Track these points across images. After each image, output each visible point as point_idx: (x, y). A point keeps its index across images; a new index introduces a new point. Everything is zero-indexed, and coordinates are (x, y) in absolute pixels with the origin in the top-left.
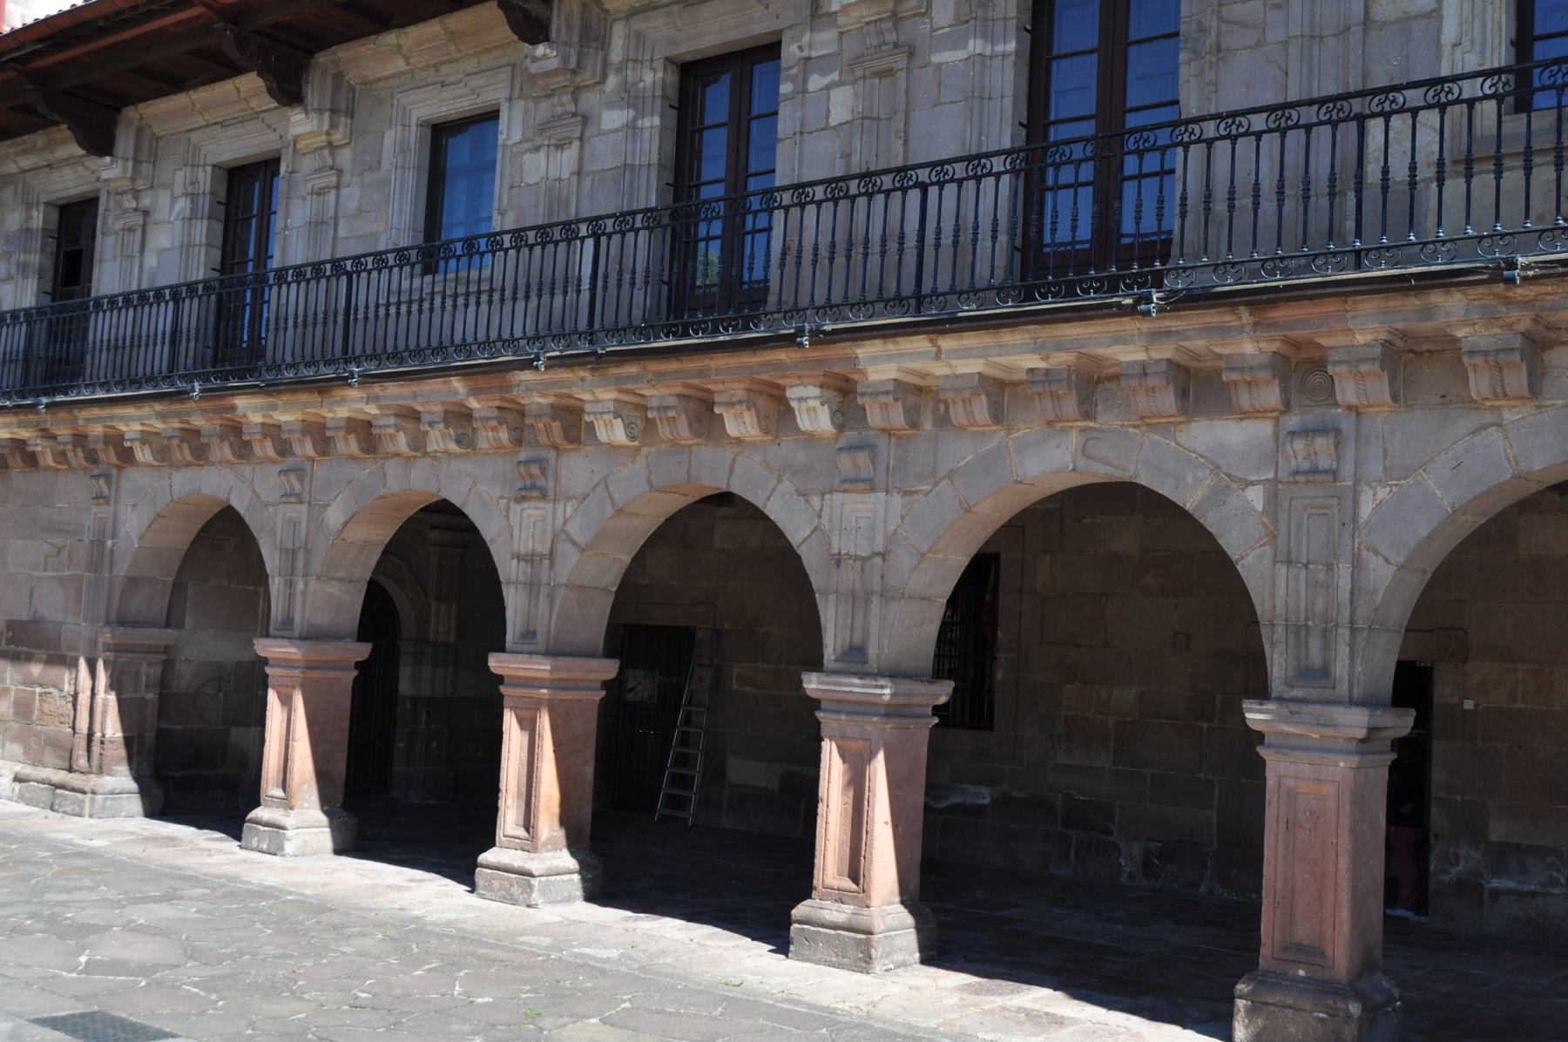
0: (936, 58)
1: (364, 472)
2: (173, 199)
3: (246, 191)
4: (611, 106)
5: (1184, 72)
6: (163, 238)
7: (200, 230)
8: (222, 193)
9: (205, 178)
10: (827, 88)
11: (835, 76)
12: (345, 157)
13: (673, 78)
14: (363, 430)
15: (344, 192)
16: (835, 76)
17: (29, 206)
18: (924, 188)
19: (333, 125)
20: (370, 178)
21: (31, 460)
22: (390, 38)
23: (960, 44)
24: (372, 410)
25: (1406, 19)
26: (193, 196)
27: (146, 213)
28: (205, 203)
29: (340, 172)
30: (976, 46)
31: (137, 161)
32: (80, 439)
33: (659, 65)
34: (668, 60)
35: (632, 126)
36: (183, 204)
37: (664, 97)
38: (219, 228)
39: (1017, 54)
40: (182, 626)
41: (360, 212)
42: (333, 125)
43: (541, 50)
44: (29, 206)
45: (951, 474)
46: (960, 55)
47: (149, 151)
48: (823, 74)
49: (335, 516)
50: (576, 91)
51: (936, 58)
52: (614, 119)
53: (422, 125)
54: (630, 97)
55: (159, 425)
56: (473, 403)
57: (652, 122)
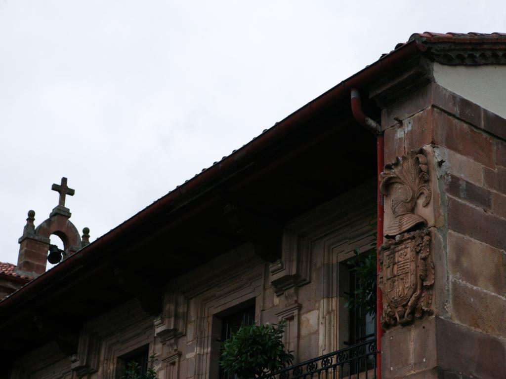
25: (310, 334)
39: (212, 353)
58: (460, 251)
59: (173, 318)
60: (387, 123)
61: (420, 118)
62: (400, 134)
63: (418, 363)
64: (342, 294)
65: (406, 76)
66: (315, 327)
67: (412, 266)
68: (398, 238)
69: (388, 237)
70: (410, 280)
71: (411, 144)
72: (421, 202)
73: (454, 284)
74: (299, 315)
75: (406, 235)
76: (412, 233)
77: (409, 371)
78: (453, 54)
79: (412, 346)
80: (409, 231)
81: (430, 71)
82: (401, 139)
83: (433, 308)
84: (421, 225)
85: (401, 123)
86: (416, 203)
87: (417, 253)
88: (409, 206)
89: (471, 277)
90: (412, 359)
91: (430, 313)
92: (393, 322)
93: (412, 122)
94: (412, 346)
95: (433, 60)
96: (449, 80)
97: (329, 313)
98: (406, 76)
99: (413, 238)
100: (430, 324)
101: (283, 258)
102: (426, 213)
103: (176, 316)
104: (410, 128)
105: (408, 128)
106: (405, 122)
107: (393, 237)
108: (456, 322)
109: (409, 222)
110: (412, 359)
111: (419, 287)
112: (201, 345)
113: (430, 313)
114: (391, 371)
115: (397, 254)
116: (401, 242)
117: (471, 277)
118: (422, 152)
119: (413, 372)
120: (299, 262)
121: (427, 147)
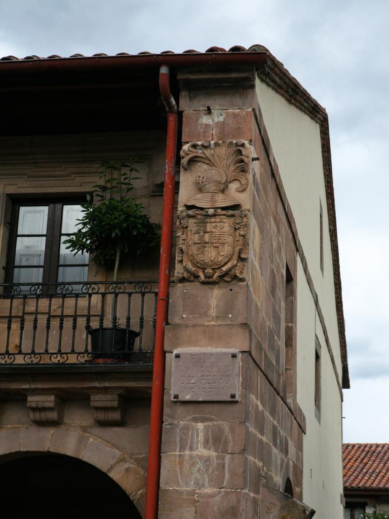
60: (187, 106)
61: (235, 116)
62: (205, 120)
63: (222, 316)
65: (234, 75)
67: (230, 239)
68: (211, 211)
70: (227, 250)
71: (222, 135)
72: (234, 186)
76: (231, 212)
77: (209, 321)
79: (213, 302)
80: (223, 209)
82: (207, 126)
83: (244, 276)
84: (236, 207)
85: (209, 111)
86: (227, 186)
87: (235, 229)
88: (222, 187)
90: (213, 312)
91: (242, 280)
92: (192, 278)
93: (224, 115)
94: (213, 302)
96: (264, 96)
98: (234, 75)
99: (233, 216)
100: (237, 287)
102: (245, 200)
104: (221, 119)
105: (218, 117)
106: (215, 112)
107: (202, 209)
109: (222, 201)
110: (213, 312)
111: (236, 256)
113: (242, 280)
114: (183, 318)
115: (208, 225)
116: (214, 215)
118: (243, 145)
119: (213, 323)
121: (246, 142)
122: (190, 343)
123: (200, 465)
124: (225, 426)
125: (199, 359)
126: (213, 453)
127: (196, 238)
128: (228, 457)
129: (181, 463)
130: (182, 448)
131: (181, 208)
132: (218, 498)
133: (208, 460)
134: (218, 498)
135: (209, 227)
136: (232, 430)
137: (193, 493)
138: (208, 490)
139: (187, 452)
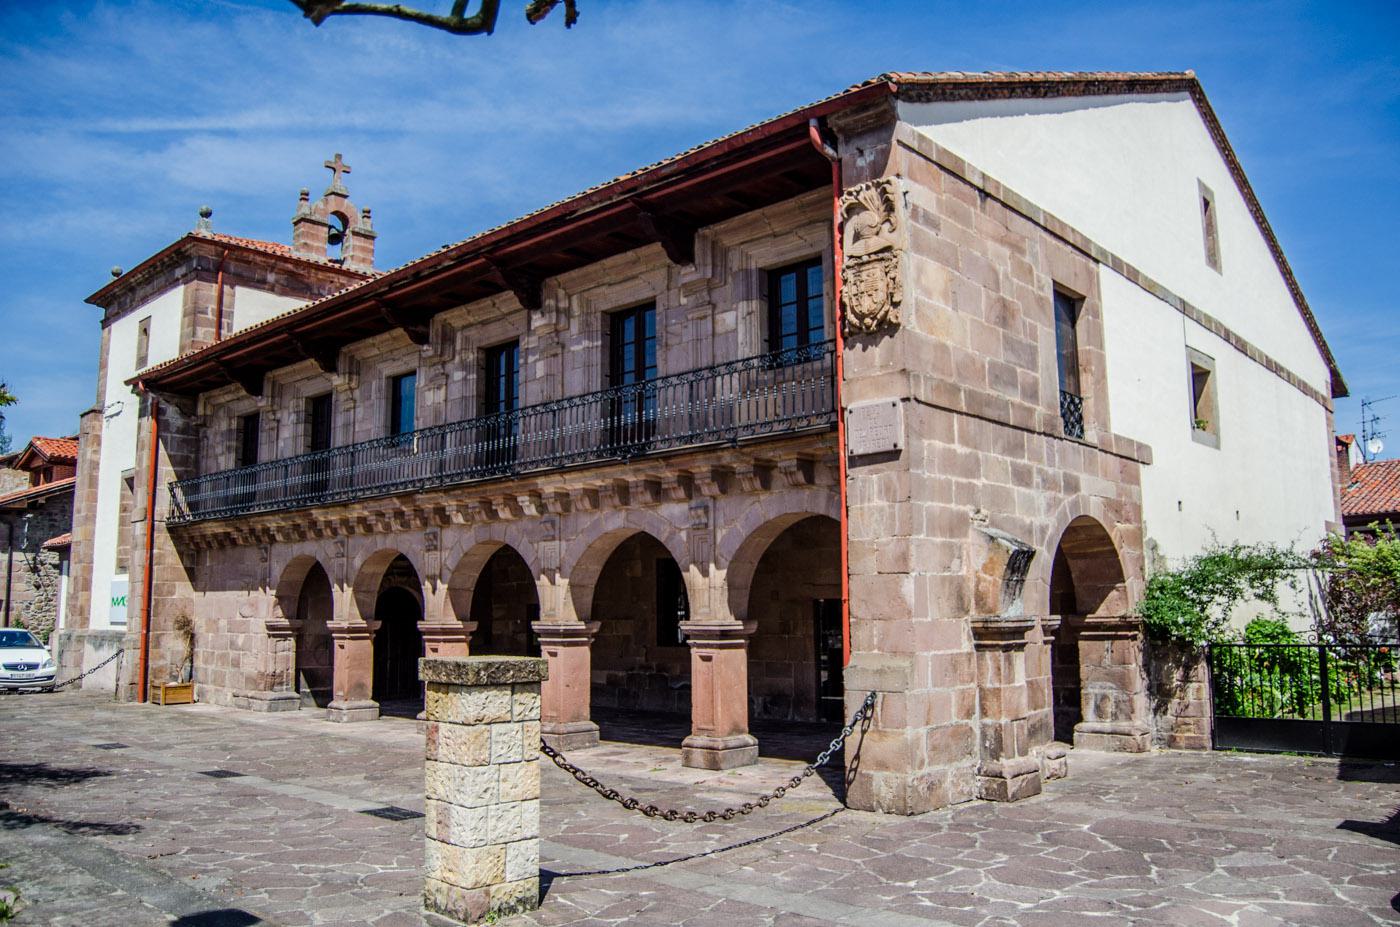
0: (572, 349)
1: (368, 541)
2: (289, 414)
3: (319, 412)
4: (457, 369)
5: (658, 353)
6: (286, 433)
7: (301, 427)
8: (311, 410)
9: (302, 404)
10: (535, 361)
11: (537, 357)
12: (357, 393)
13: (482, 356)
14: (362, 520)
15: (358, 410)
16: (537, 357)
17: (230, 419)
18: (554, 411)
19: (350, 380)
20: (367, 403)
21: (234, 542)
22: (370, 341)
23: (579, 343)
24: (366, 513)
25: (727, 332)
26: (297, 413)
27: (278, 421)
28: (302, 415)
29: (355, 401)
30: (586, 343)
31: (273, 397)
32: (252, 531)
33: (475, 351)
34: (479, 348)
35: (465, 379)
36: (293, 417)
37: (478, 365)
38: (310, 427)
39: (602, 346)
40: (306, 618)
41: (364, 419)
42: (350, 380)
43: (425, 347)
44: (230, 419)
45: (582, 532)
46: (581, 347)
47: (278, 392)
48: (534, 355)
49: (358, 562)
50: (444, 364)
51: (572, 349)
52: (458, 375)
53: (388, 378)
54: (464, 366)
55: (283, 524)
56: (404, 509)
57: (473, 376)
58: (920, 270)
59: (554, 314)
64: (761, 297)
66: (733, 326)
68: (865, 258)
69: (851, 257)
73: (916, 299)
74: (713, 315)
75: (873, 257)
76: (881, 255)
78: (913, 93)
80: (876, 253)
81: (894, 109)
82: (862, 168)
84: (888, 249)
85: (861, 153)
89: (928, 293)
95: (897, 98)
97: (749, 314)
101: (697, 262)
103: (558, 311)
104: (872, 158)
106: (866, 153)
107: (860, 257)
108: (917, 331)
112: (590, 338)
116: (869, 262)
117: (928, 293)
118: (888, 182)
120: (714, 266)
121: (893, 178)
122: (862, 396)
123: (876, 515)
124: (894, 475)
125: (867, 411)
126: (885, 504)
127: (854, 290)
128: (897, 505)
129: (862, 515)
130: (862, 501)
131: (846, 259)
132: (891, 546)
133: (881, 510)
134: (891, 546)
135: (864, 276)
136: (899, 478)
137: (872, 543)
138: (883, 540)
139: (866, 504)
